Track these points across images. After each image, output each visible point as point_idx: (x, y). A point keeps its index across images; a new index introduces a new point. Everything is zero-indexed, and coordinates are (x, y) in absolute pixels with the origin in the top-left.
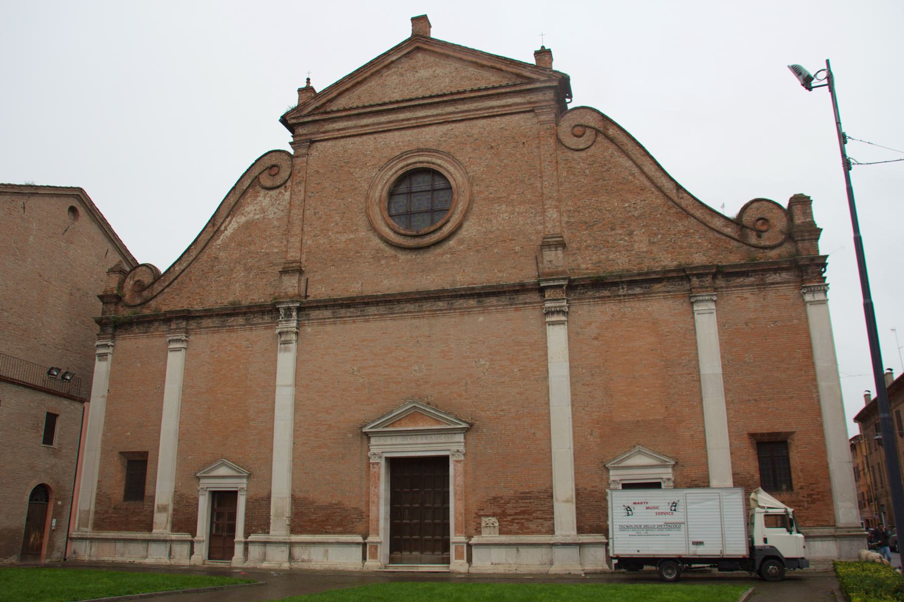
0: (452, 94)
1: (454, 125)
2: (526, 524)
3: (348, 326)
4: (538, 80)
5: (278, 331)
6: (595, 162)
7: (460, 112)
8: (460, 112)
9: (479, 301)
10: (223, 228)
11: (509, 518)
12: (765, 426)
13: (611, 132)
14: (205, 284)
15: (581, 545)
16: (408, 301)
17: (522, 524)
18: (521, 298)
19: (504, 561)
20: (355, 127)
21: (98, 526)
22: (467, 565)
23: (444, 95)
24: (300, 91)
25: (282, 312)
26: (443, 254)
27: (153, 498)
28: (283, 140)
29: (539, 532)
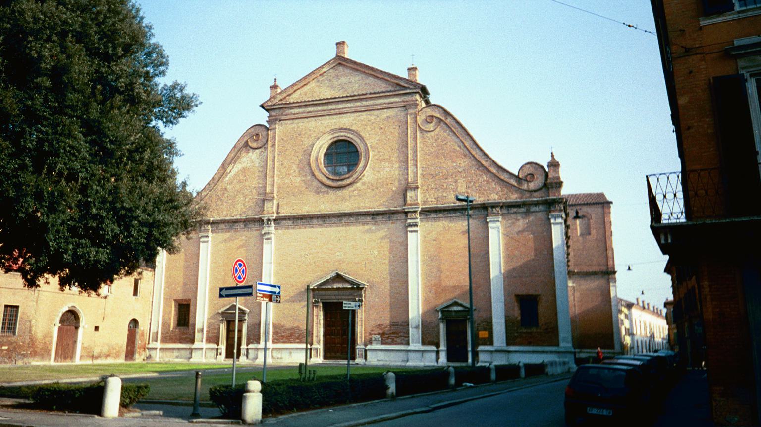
0: (359, 95)
1: (360, 113)
2: (395, 339)
3: (302, 230)
4: (409, 88)
5: (263, 233)
6: (438, 138)
7: (364, 106)
8: (364, 106)
9: (372, 218)
10: (228, 171)
11: (387, 336)
12: (523, 291)
13: (449, 120)
14: (220, 203)
15: (424, 351)
16: (334, 217)
17: (393, 339)
18: (396, 216)
19: (383, 359)
20: (304, 113)
21: (164, 341)
22: (364, 360)
23: (354, 96)
24: (271, 87)
25: (265, 222)
26: (353, 191)
27: (194, 325)
28: (262, 117)
29: (402, 344)
